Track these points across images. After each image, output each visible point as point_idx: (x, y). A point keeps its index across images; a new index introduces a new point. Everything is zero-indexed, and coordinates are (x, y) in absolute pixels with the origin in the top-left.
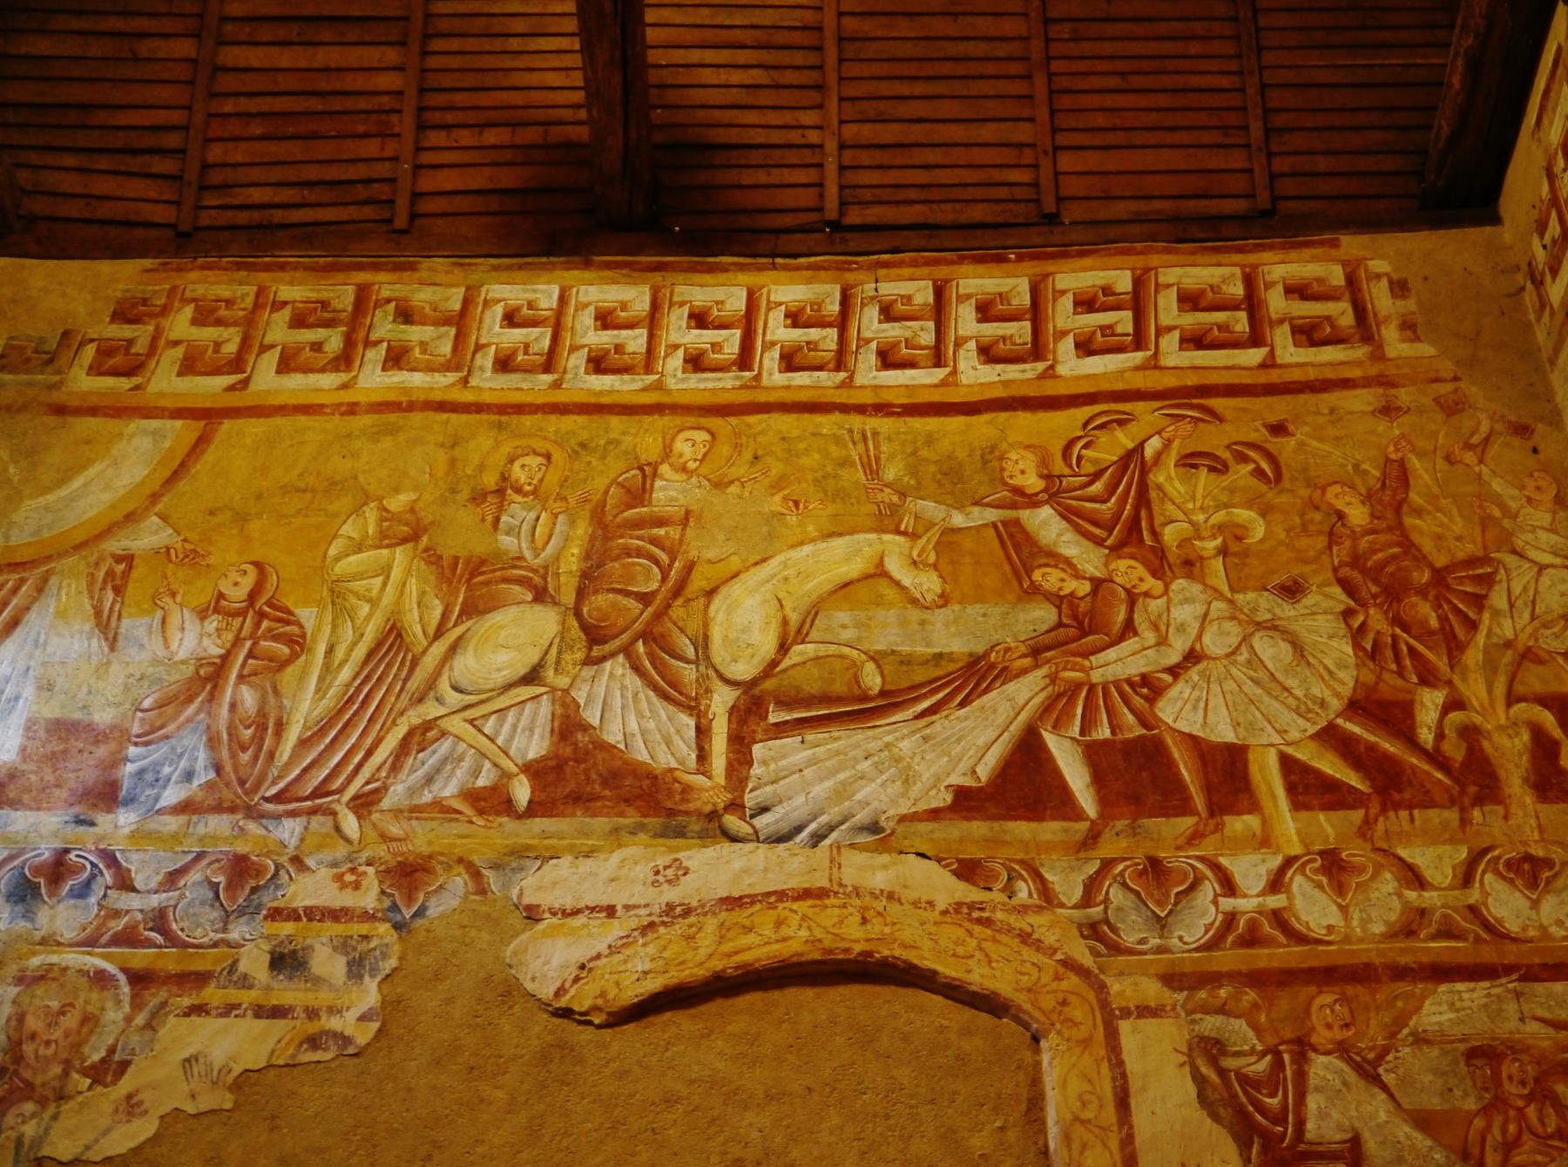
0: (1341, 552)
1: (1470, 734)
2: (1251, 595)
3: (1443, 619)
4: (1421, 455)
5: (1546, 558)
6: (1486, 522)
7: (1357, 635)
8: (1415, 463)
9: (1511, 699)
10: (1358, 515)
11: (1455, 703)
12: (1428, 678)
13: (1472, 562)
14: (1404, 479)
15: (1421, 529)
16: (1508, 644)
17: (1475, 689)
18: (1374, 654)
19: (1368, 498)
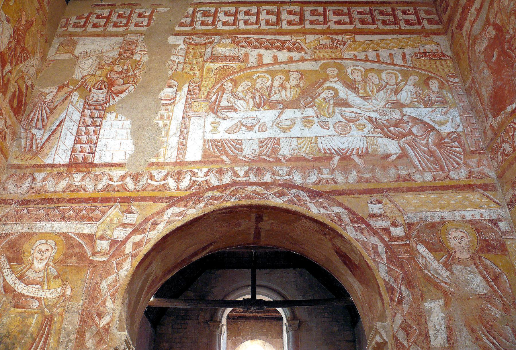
0: (17, 25)
1: (9, 79)
2: (3, 13)
3: (19, 56)
4: (36, 25)
5: (35, 65)
6: (33, 49)
7: (10, 42)
8: (34, 24)
9: (16, 82)
10: (23, 22)
11: (10, 72)
12: (11, 63)
13: (28, 52)
14: (31, 25)
15: (28, 37)
16: (22, 72)
17: (14, 73)
18: (9, 48)
19: (26, 21)
